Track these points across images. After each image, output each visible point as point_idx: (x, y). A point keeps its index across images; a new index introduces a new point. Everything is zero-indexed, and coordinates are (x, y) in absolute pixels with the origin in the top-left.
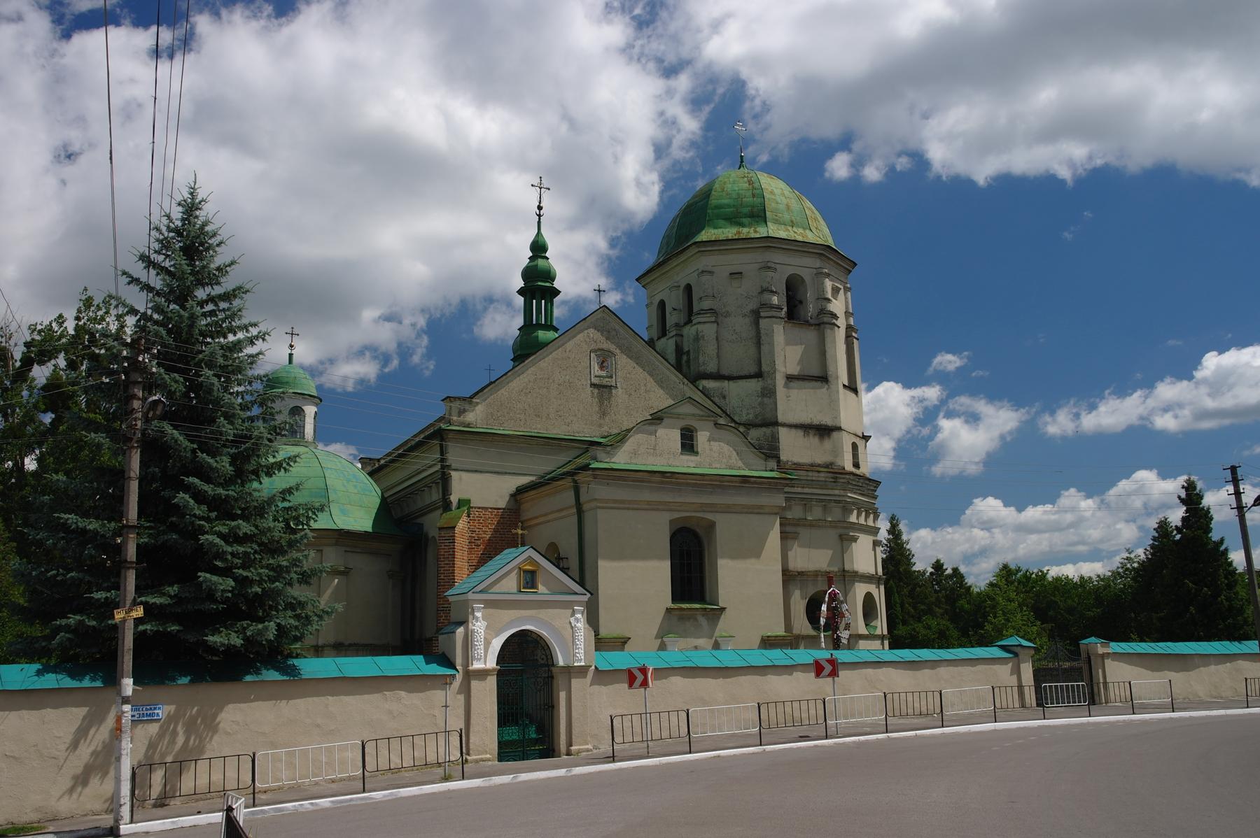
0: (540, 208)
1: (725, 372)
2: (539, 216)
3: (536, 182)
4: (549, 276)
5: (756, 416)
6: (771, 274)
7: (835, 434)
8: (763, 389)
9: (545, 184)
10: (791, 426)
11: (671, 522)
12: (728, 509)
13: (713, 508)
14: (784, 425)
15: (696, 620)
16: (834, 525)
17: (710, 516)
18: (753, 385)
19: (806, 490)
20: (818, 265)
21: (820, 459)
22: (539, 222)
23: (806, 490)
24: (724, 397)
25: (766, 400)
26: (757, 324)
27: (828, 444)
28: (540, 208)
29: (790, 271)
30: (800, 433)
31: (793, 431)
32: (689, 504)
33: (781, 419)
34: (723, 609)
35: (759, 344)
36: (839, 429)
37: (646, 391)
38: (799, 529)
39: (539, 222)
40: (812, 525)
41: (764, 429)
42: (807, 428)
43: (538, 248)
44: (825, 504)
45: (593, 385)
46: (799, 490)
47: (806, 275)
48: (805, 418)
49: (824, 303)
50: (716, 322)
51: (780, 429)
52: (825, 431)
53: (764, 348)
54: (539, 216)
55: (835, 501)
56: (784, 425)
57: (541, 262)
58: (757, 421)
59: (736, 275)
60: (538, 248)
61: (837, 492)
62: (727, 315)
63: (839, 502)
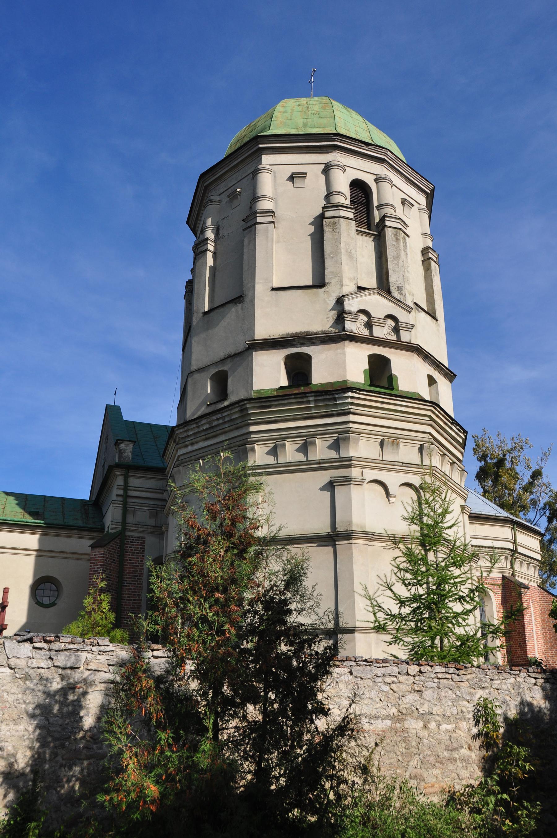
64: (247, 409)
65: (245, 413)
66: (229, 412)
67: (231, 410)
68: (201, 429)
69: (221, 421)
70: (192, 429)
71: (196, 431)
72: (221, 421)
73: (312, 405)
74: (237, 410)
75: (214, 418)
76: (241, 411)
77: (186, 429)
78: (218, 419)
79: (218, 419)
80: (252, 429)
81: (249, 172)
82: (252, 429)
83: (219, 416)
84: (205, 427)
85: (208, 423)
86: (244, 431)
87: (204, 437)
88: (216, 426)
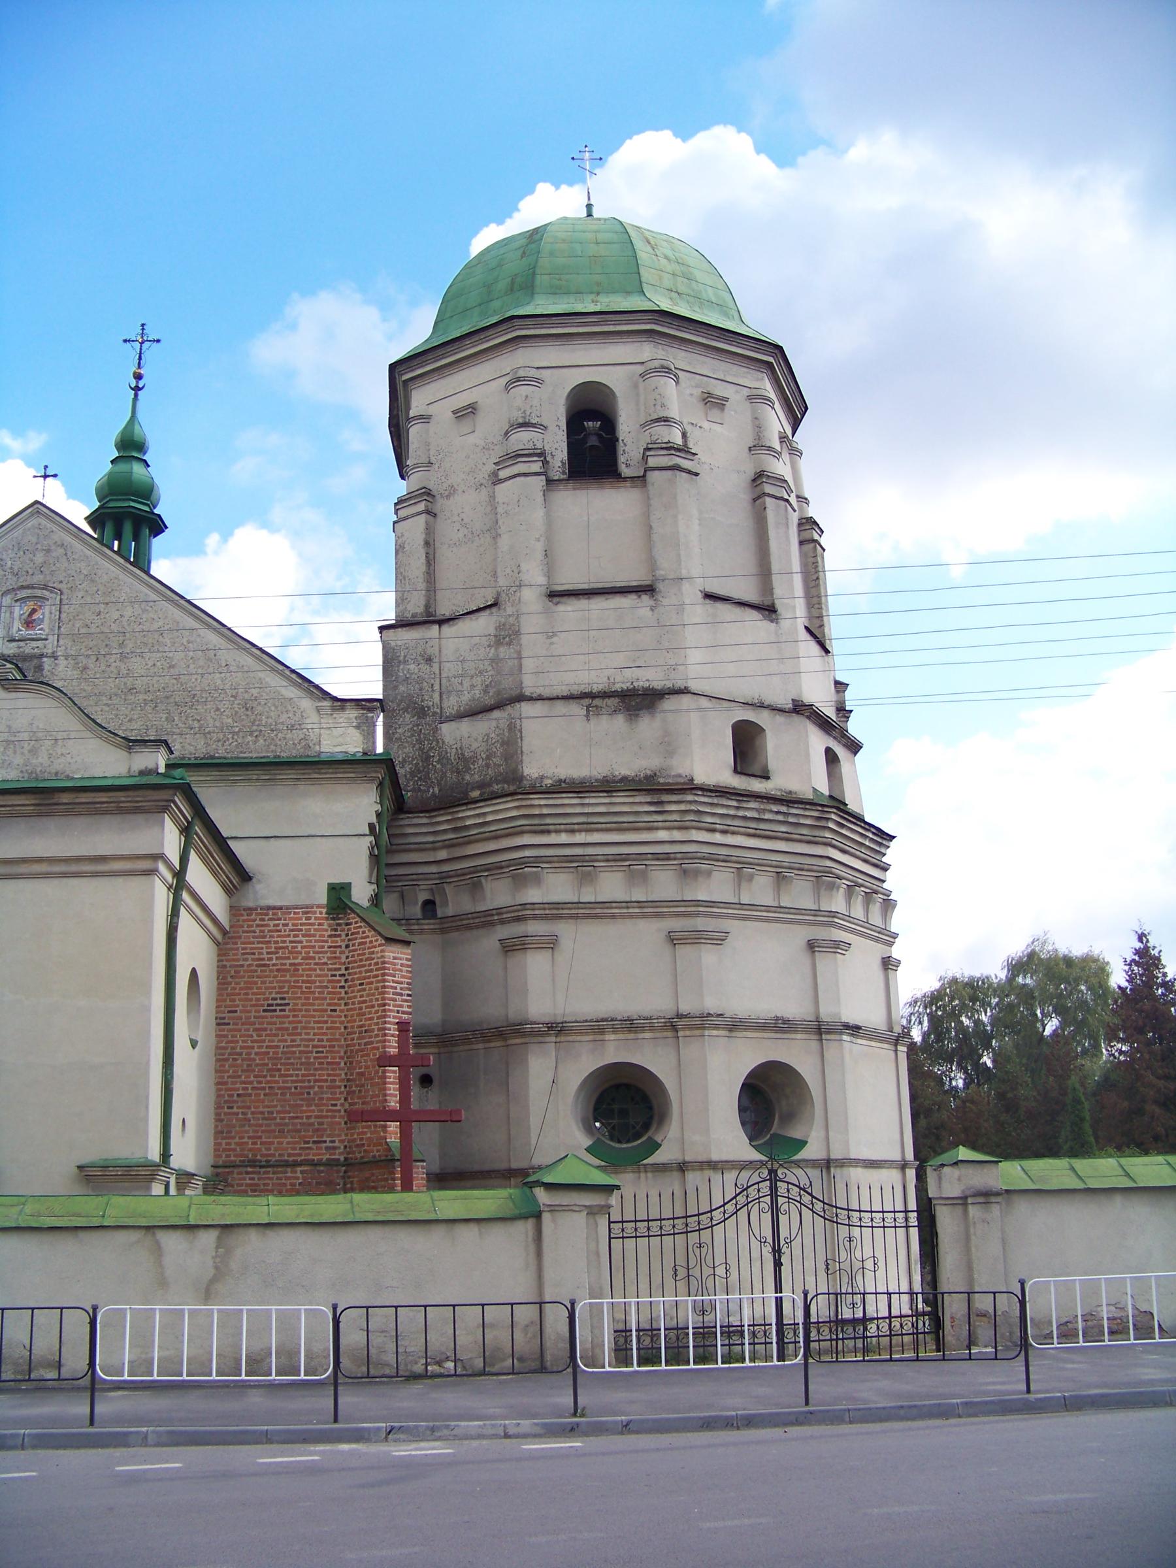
0: (138, 377)
1: (444, 610)
2: (137, 389)
3: (134, 333)
4: (146, 493)
5: (486, 691)
6: (523, 390)
7: (669, 704)
8: (501, 627)
14: (540, 698)
16: (651, 909)
18: (484, 624)
19: (580, 838)
21: (628, 763)
23: (580, 838)
24: (429, 660)
25: (503, 651)
26: (493, 497)
27: (648, 726)
28: (138, 377)
30: (577, 709)
31: (560, 707)
35: (496, 537)
38: (565, 930)
41: (496, 714)
42: (591, 699)
43: (131, 447)
44: (632, 864)
46: (564, 838)
50: (428, 512)
51: (526, 708)
52: (639, 701)
53: (504, 542)
54: (137, 389)
55: (656, 856)
56: (540, 698)
57: (137, 469)
58: (489, 700)
59: (467, 412)
60: (131, 447)
61: (662, 835)
62: (451, 492)
63: (667, 856)
67: (806, 809)
68: (741, 813)
69: (780, 818)
71: (732, 812)
72: (780, 818)
75: (775, 808)
77: (715, 801)
78: (778, 813)
79: (778, 813)
83: (784, 809)
84: (749, 814)
85: (757, 810)
87: (753, 831)
88: (767, 820)
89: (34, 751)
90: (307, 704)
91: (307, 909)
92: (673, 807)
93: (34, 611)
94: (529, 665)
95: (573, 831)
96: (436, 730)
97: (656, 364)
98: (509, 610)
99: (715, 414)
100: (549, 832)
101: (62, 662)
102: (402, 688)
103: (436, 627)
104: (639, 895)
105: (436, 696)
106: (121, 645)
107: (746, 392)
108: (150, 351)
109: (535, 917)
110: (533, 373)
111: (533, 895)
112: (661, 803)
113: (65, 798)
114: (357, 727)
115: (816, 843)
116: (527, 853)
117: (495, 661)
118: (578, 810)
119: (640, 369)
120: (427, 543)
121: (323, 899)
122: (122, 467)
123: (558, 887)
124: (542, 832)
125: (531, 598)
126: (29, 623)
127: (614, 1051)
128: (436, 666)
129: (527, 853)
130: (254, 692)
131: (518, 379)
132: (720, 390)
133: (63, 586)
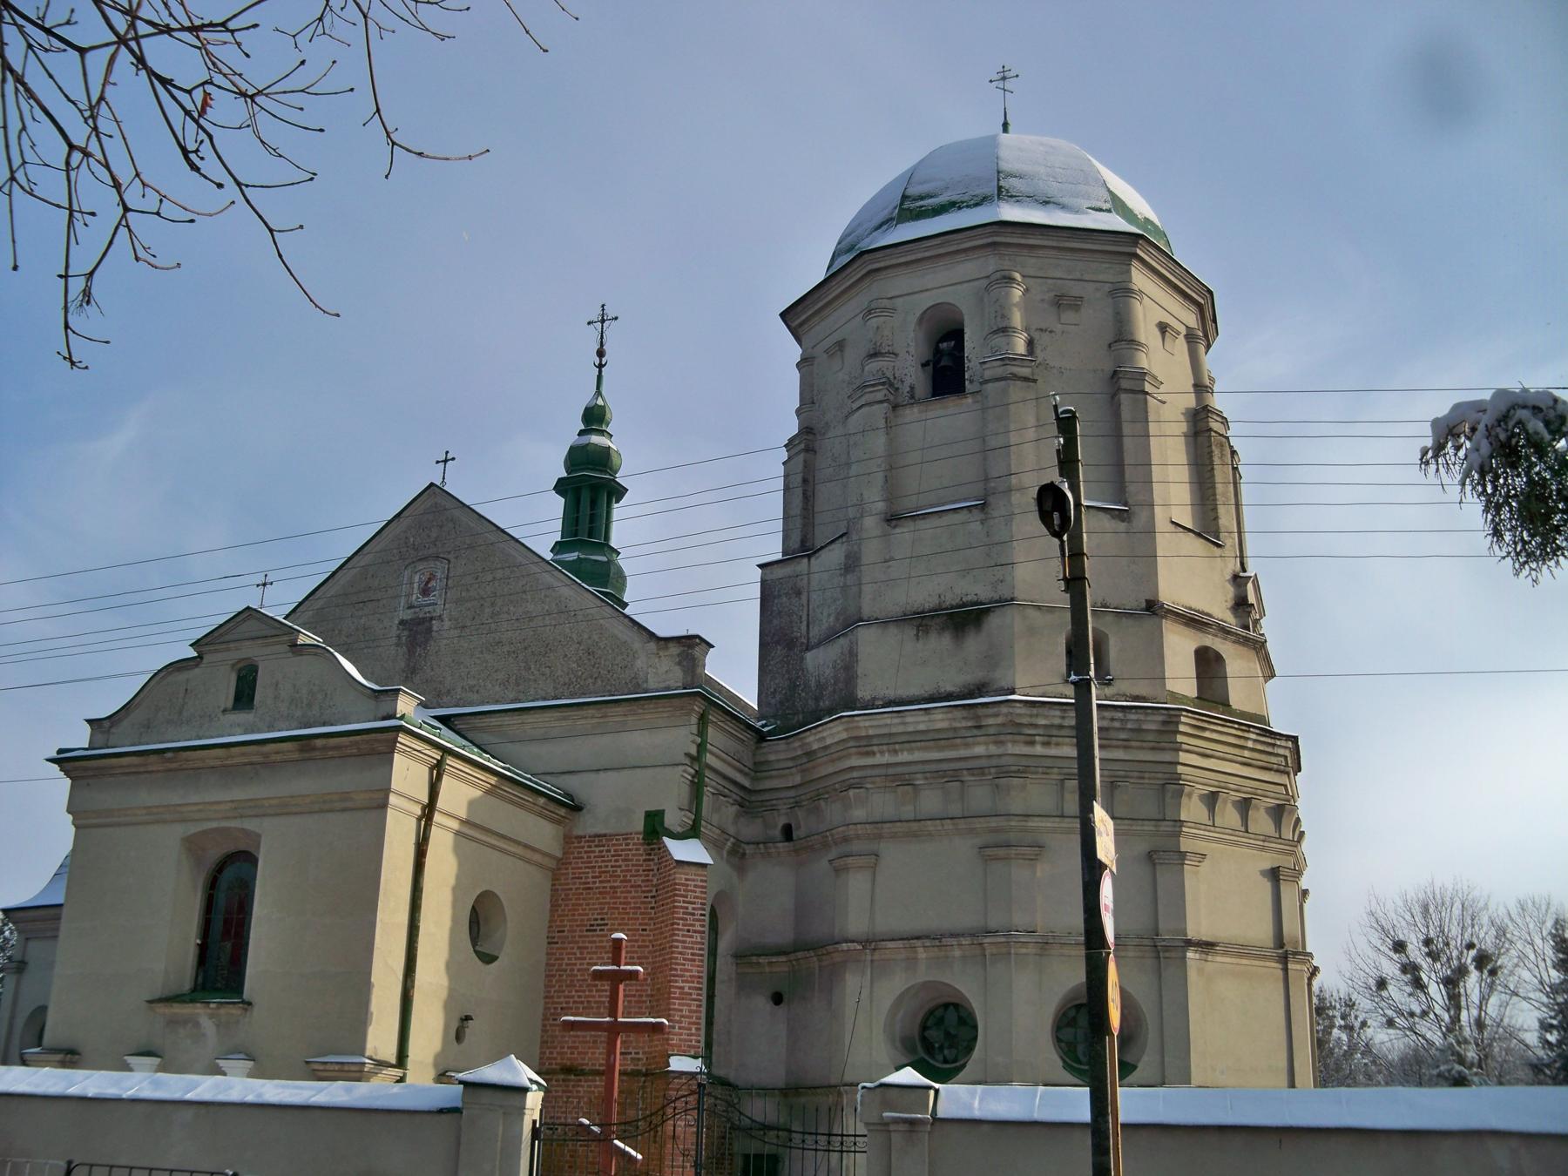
0: (601, 353)
2: (600, 366)
3: (595, 315)
5: (837, 619)
7: (994, 621)
9: (610, 313)
10: (885, 623)
11: (193, 845)
12: (284, 809)
13: (257, 809)
15: (197, 1025)
17: (250, 825)
20: (991, 269)
22: (600, 377)
24: (798, 593)
27: (974, 644)
28: (601, 353)
29: (927, 301)
31: (893, 630)
32: (214, 804)
33: (866, 612)
34: (250, 1004)
36: (1006, 602)
37: (493, 615)
38: (885, 848)
39: (600, 377)
40: (914, 829)
42: (921, 621)
43: (594, 418)
45: (402, 622)
46: (887, 758)
47: (963, 300)
48: (925, 592)
49: (999, 340)
52: (963, 619)
57: (596, 439)
60: (594, 418)
61: (979, 750)
63: (981, 771)
64: (1178, 723)
65: (1171, 727)
66: (1142, 717)
70: (1046, 717)
71: (1057, 721)
72: (1117, 724)
73: (1250, 744)
74: (1161, 718)
76: (1164, 723)
79: (1113, 719)
80: (1183, 757)
81: (1101, 278)
82: (1183, 757)
86: (1167, 757)
89: (310, 705)
90: (637, 643)
91: (627, 836)
92: (991, 721)
93: (430, 580)
94: (867, 590)
95: (896, 752)
96: (802, 659)
97: (998, 275)
98: (854, 537)
99: (1069, 316)
100: (874, 753)
101: (447, 624)
102: (775, 622)
103: (805, 560)
104: (955, 809)
105: (804, 627)
106: (493, 604)
107: (1107, 287)
108: (611, 330)
109: (858, 837)
110: (885, 303)
111: (859, 814)
112: (978, 718)
113: (319, 742)
114: (679, 663)
115: (1163, 749)
116: (855, 774)
117: (844, 588)
118: (901, 729)
119: (985, 282)
120: (805, 481)
121: (640, 827)
122: (585, 440)
123: (880, 804)
124: (868, 754)
125: (871, 524)
126: (425, 591)
127: (926, 969)
128: (804, 597)
129: (855, 774)
130: (596, 637)
131: (870, 312)
132: (1076, 290)
133: (450, 557)
